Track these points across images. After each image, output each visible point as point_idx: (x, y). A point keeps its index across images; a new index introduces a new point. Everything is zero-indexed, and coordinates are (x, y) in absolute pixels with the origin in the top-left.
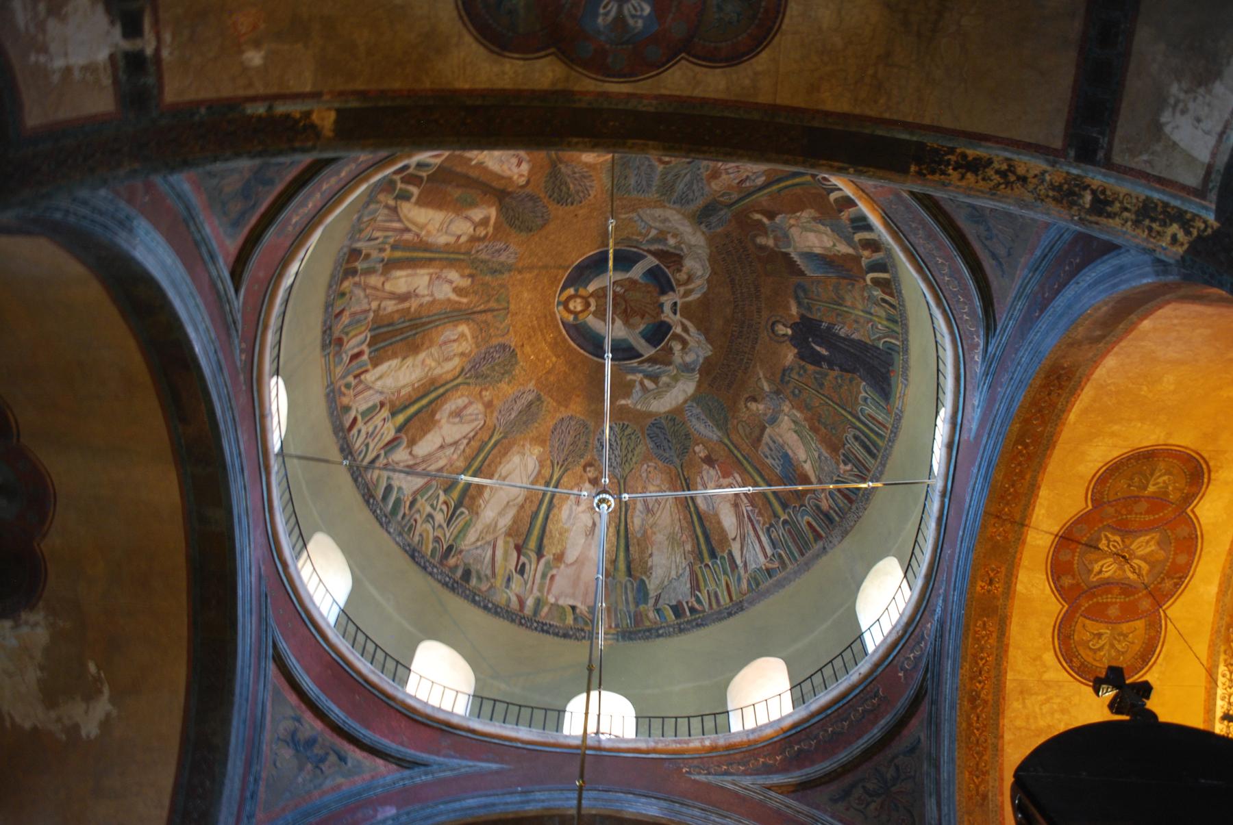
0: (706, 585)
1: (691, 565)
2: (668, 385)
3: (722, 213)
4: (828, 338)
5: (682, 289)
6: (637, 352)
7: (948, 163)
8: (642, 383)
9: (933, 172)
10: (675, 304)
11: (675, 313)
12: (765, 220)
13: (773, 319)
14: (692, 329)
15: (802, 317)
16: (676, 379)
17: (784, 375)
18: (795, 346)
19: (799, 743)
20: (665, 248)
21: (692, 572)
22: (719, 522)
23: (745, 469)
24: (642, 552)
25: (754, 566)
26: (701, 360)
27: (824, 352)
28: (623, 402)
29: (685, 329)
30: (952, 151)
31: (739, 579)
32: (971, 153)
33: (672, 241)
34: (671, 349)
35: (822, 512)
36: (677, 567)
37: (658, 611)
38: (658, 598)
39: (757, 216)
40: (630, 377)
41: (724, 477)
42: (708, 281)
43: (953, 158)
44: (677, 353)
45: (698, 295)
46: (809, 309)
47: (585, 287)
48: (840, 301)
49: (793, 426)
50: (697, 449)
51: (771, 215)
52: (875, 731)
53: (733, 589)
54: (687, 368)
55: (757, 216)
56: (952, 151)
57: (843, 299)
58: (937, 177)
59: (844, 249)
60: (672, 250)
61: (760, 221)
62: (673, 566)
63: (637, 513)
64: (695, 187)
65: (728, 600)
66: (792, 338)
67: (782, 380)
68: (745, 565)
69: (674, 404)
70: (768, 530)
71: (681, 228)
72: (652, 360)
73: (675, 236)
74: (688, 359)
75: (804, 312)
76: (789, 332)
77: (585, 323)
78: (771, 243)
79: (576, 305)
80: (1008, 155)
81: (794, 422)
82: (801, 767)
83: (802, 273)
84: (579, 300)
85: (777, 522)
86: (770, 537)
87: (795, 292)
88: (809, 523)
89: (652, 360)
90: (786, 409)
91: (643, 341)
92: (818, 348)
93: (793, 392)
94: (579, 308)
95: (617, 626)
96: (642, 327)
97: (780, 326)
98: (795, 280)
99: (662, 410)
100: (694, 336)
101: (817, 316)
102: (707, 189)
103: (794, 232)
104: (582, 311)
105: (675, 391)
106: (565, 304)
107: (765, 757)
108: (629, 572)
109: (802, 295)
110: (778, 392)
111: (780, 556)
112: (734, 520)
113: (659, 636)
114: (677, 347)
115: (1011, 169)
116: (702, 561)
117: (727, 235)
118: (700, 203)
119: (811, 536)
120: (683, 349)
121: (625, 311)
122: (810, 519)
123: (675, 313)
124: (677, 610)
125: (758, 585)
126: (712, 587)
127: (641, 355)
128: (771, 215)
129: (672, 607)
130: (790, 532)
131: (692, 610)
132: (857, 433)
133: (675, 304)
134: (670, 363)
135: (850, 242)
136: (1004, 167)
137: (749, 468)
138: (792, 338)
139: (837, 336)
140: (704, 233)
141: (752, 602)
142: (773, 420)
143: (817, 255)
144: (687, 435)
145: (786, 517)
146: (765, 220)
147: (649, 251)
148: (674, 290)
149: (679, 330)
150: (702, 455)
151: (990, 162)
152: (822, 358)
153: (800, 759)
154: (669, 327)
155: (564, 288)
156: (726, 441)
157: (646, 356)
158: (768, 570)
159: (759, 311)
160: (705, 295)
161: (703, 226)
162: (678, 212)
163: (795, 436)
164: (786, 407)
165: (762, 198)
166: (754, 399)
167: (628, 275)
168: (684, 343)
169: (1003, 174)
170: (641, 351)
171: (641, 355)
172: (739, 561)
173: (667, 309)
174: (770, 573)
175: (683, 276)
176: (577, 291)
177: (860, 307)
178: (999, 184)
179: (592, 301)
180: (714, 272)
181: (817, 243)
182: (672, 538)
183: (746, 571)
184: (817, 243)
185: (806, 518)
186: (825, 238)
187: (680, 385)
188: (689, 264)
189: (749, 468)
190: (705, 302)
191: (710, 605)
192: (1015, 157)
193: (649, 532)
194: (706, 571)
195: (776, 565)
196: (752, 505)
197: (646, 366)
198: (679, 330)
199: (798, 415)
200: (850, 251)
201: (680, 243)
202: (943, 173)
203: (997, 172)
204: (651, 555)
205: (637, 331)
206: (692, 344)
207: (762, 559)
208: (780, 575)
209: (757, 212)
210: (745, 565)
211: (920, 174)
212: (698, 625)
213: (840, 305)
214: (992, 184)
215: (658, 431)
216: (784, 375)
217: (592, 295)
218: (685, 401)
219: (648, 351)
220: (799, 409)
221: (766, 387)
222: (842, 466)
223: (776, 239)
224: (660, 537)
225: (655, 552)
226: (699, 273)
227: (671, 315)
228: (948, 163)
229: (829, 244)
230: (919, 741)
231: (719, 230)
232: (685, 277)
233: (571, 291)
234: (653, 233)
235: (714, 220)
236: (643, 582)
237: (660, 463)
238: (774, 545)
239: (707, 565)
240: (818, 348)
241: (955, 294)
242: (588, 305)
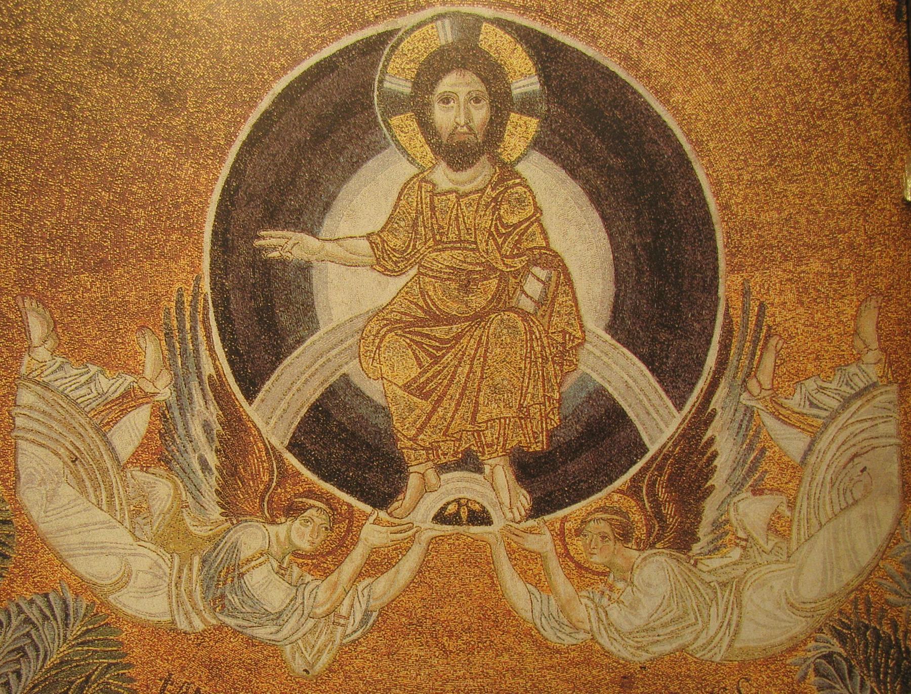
2: (139, 512)
5: (542, 541)
6: (263, 376)
8: (128, 401)
10: (480, 518)
11: (441, 518)
14: (384, 587)
16: (173, 536)
20: (718, 480)
26: (262, 633)
28: (37, 328)
29: (377, 564)
33: (752, 512)
34: (293, 510)
40: (151, 351)
42: (589, 655)
44: (280, 530)
47: (538, 144)
54: (223, 578)
60: (710, 509)
69: (67, 542)
72: (235, 436)
77: (374, 149)
79: (458, 105)
84: (481, 114)
89: (235, 436)
91: (313, 393)
94: (444, 118)
96: (373, 389)
99: (32, 498)
100: (353, 598)
104: (426, 126)
105: (121, 536)
106: (465, 55)
114: (303, 532)
120: (296, 553)
121: (438, 319)
123: (441, 518)
127: (250, 396)
133: (480, 518)
134: (231, 509)
147: (703, 417)
155: (544, 51)
157: (252, 412)
167: (589, 324)
168: (322, 560)
170: (271, 388)
171: (250, 396)
173: (458, 486)
176: (527, 106)
179: (479, 174)
187: (146, 560)
188: (656, 571)
190: (497, 617)
197: (204, 411)
198: (374, 532)
201: (746, 543)
205: (352, 368)
206: (321, 593)
217: (507, 172)
218: (85, 586)
219: (274, 415)
226: (615, 613)
227: (431, 504)
232: (597, 560)
233: (525, 80)
234: (792, 442)
242: (458, 155)
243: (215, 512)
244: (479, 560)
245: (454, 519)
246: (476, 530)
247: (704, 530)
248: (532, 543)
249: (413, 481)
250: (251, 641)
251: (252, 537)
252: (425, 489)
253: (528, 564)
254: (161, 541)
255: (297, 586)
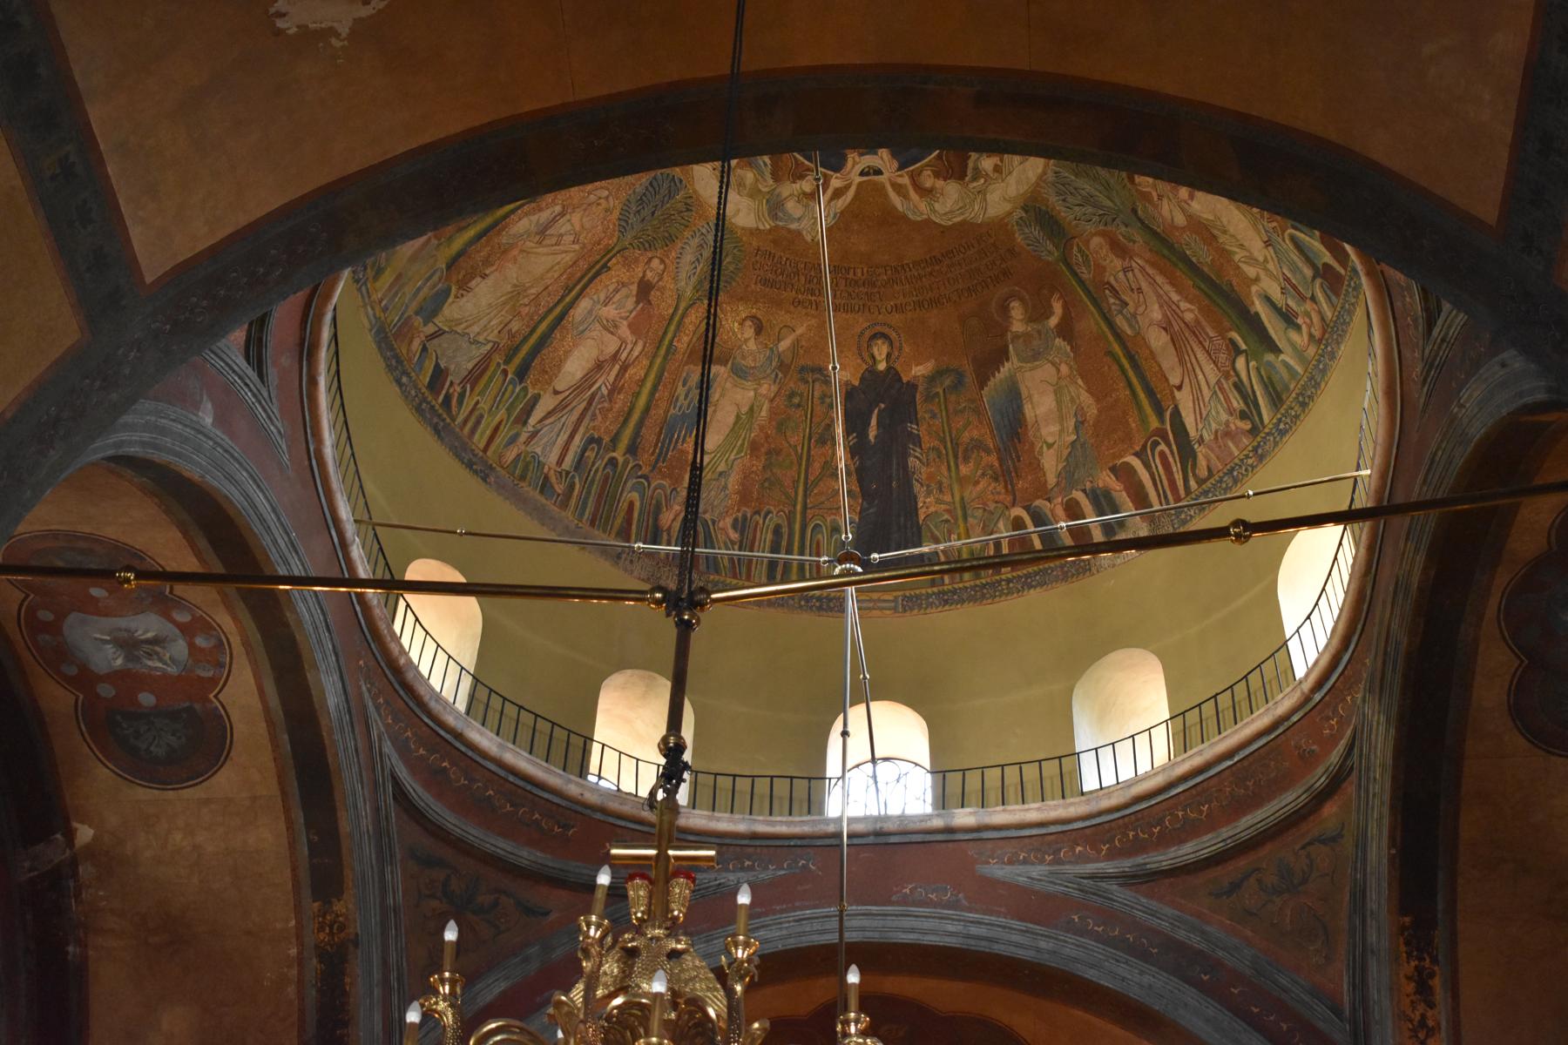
0: (482, 393)
1: (496, 347)
3: (1050, 247)
4: (897, 439)
5: (906, 180)
7: (1421, 959)
9: (1407, 943)
10: (878, 172)
11: (862, 174)
12: (1053, 321)
13: (893, 335)
15: (912, 387)
17: (813, 370)
18: (862, 379)
19: (452, 764)
21: (487, 357)
22: (568, 353)
23: (655, 356)
24: (487, 262)
25: (538, 450)
26: (793, 226)
27: (872, 434)
29: (838, 193)
30: (1435, 961)
31: (513, 440)
32: (1437, 983)
34: (802, 177)
35: (656, 519)
36: (485, 328)
37: (424, 349)
38: (439, 333)
39: (1058, 307)
41: (630, 326)
43: (1427, 963)
45: (900, 208)
46: (929, 398)
48: (963, 452)
49: (744, 410)
50: (655, 263)
51: (1066, 330)
52: (525, 854)
53: (498, 440)
54: (776, 207)
55: (1058, 307)
56: (1435, 961)
57: (966, 459)
58: (1403, 948)
59: (1051, 465)
61: (1048, 313)
62: (483, 323)
63: (534, 218)
64: (1090, 210)
65: (482, 446)
66: (872, 371)
67: (803, 369)
68: (534, 434)
70: (591, 440)
71: (1012, 180)
73: (997, 169)
74: (790, 205)
75: (920, 388)
76: (882, 366)
78: (1018, 326)
80: (1444, 1024)
81: (751, 409)
82: (427, 785)
83: (982, 383)
85: (607, 450)
86: (584, 451)
87: (948, 371)
88: (631, 504)
90: (764, 390)
92: (874, 422)
93: (792, 395)
95: (385, 309)
97: (885, 349)
98: (968, 369)
101: (922, 409)
102: (1090, 228)
103: (1046, 371)
107: (415, 734)
108: (452, 264)
109: (947, 382)
110: (783, 367)
111: (572, 486)
112: (579, 375)
113: (399, 382)
114: (806, 185)
115: (1431, 1032)
116: (507, 362)
117: (1011, 251)
118: (1065, 214)
119: (619, 521)
120: (805, 194)
122: (637, 504)
123: (862, 174)
124: (439, 374)
125: (523, 478)
126: (484, 406)
128: (1066, 330)
129: (437, 365)
130: (606, 478)
131: (447, 402)
132: (785, 530)
133: (878, 172)
134: (776, 177)
135: (1068, 477)
136: (1431, 1023)
137: (658, 361)
138: (872, 371)
139: (905, 456)
140: (1010, 214)
141: (500, 487)
142: (740, 373)
143: (1020, 409)
144: (670, 239)
145: (621, 460)
146: (1053, 321)
148: (899, 169)
149: (836, 183)
150: (649, 274)
151: (1431, 1005)
152: (863, 435)
153: (435, 779)
154: (837, 169)
156: (683, 306)
158: (546, 478)
159: (898, 309)
160: (904, 217)
161: (1020, 213)
162: (1041, 177)
163: (732, 419)
164: (767, 388)
165: (1090, 323)
166: (759, 330)
169: (1423, 1022)
172: (532, 421)
173: (868, 160)
174: (545, 486)
175: (928, 181)
177: (966, 494)
178: (1411, 1021)
180: (944, 230)
181: (1041, 410)
182: (518, 291)
183: (527, 443)
184: (1041, 410)
185: (635, 496)
186: (1055, 428)
188: (952, 189)
189: (658, 361)
191: (465, 421)
192: (1443, 1034)
193: (515, 252)
194: (499, 376)
195: (560, 488)
196: (611, 392)
198: (836, 183)
199: (764, 413)
200: (1051, 479)
202: (1409, 955)
203: (1423, 1016)
204: (484, 276)
207: (553, 458)
208: (549, 504)
209: (1066, 307)
210: (534, 434)
211: (1403, 929)
212: (437, 431)
213: (956, 457)
214: (1409, 1012)
215: (664, 191)
216: (813, 370)
220: (773, 412)
221: (784, 345)
222: (729, 521)
223: (1027, 337)
224: (512, 272)
225: (489, 281)
226: (937, 206)
227: (859, 168)
228: (1421, 959)
229: (1050, 431)
230: (547, 914)
231: (1019, 238)
232: (928, 184)
235: (1036, 232)
236: (447, 292)
237: (616, 214)
238: (580, 463)
239: (505, 372)
240: (874, 422)
241: (1160, 822)
243: (771, 182)
244: (880, 189)
245: (868, 174)
246: (876, 178)
247: (969, 172)
248: (900, 180)
249: (850, 162)
250: (789, 231)
251: (788, 189)
252: (855, 163)
253: (898, 188)
254: (751, 196)
255: (806, 206)
